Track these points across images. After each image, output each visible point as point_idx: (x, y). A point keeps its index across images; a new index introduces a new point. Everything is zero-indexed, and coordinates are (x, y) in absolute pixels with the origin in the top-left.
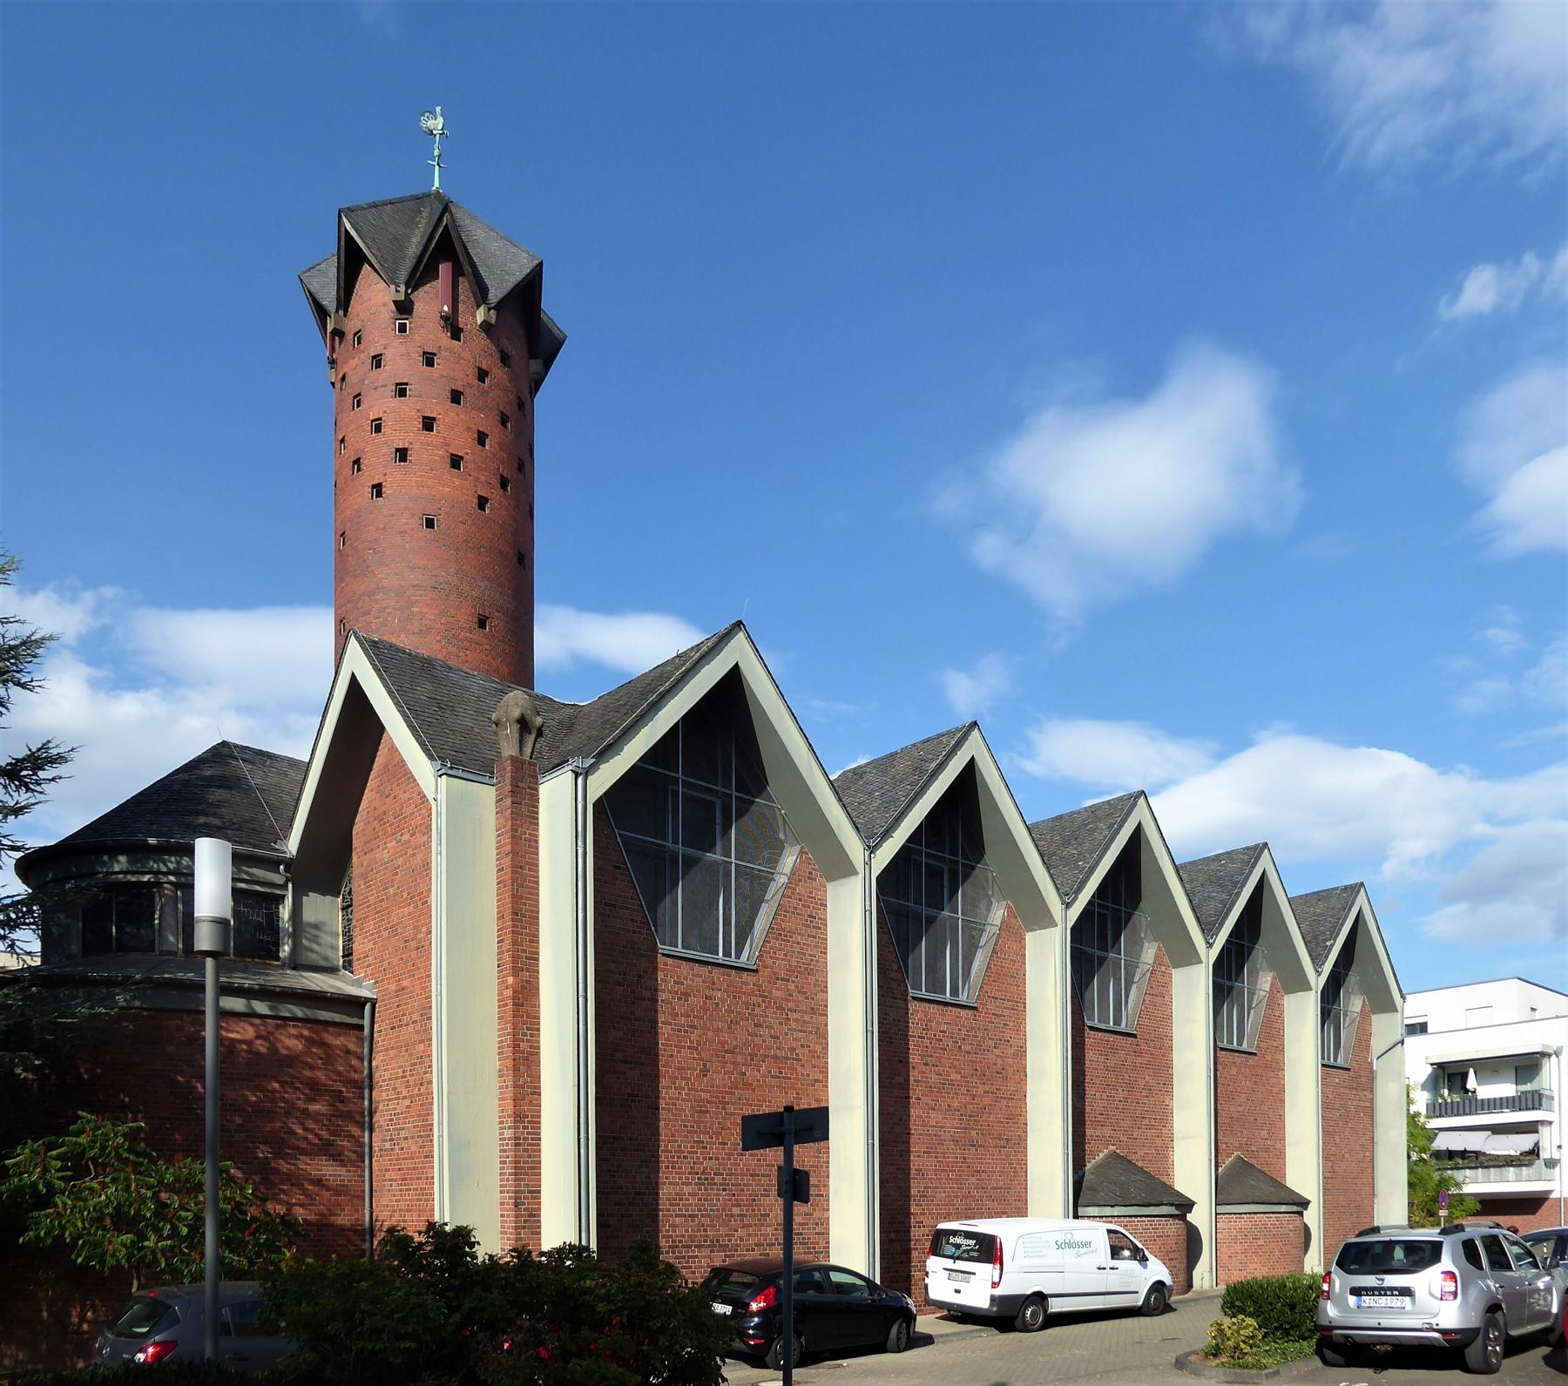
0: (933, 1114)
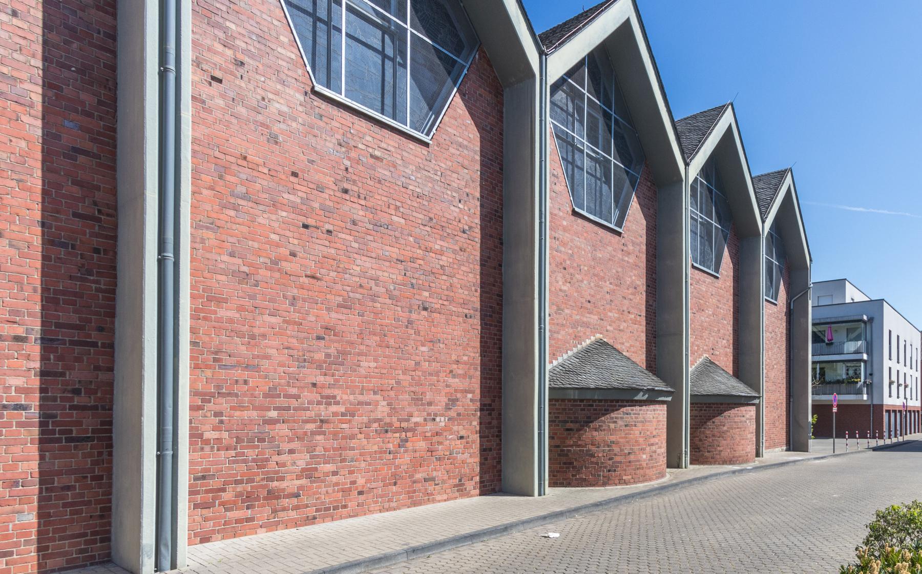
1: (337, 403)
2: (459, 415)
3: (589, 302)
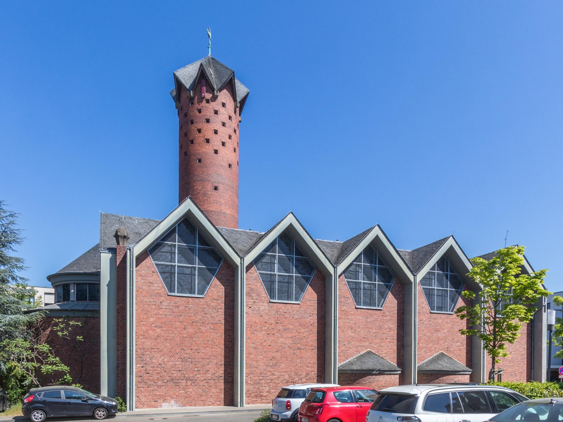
0: (281, 339)
1: (275, 375)
2: (310, 378)
3: (364, 338)
